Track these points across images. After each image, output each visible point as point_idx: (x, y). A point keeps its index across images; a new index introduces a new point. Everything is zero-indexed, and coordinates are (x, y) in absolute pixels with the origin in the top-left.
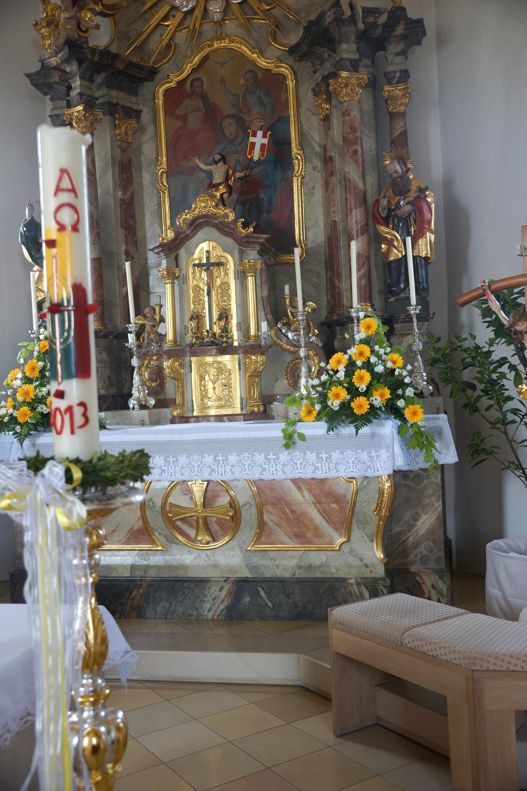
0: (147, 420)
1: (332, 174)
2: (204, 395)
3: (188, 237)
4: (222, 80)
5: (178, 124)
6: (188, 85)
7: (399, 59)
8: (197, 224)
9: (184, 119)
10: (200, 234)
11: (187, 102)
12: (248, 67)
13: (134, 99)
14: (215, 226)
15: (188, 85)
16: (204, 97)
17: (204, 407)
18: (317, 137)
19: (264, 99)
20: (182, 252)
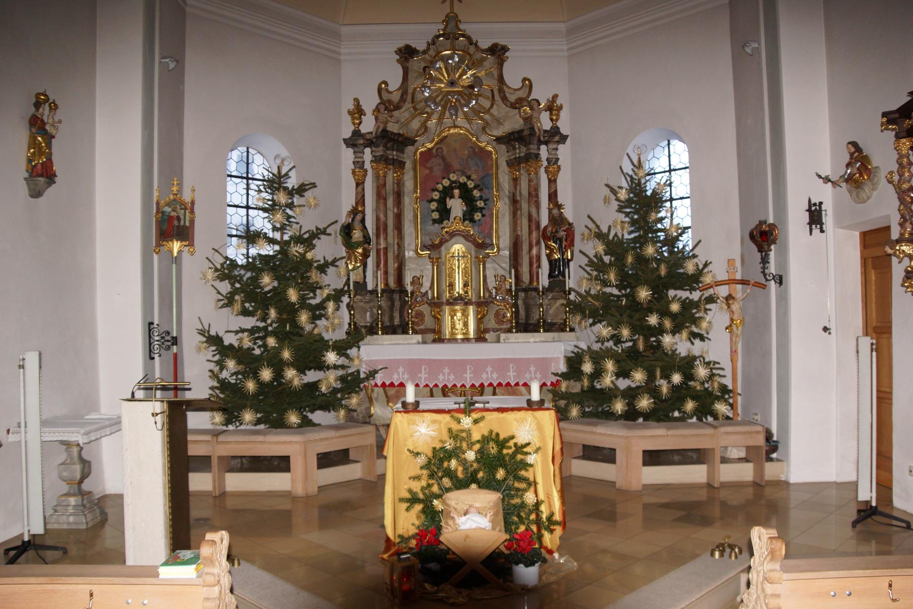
0: (420, 340)
1: (517, 210)
2: (453, 327)
3: (447, 241)
4: (455, 150)
5: (427, 172)
6: (434, 151)
7: (553, 152)
8: (452, 235)
9: (431, 169)
10: (454, 240)
11: (433, 160)
12: (470, 145)
13: (402, 155)
14: (463, 236)
15: (434, 151)
16: (444, 159)
17: (453, 334)
18: (507, 186)
19: (479, 163)
20: (443, 248)
